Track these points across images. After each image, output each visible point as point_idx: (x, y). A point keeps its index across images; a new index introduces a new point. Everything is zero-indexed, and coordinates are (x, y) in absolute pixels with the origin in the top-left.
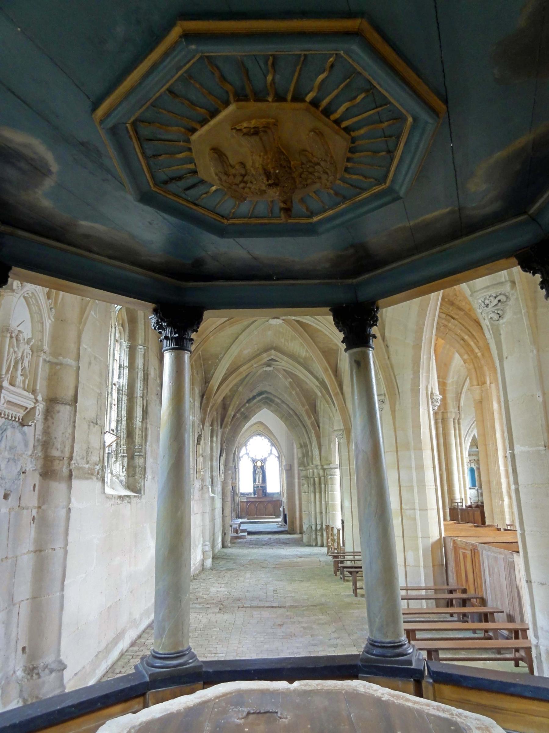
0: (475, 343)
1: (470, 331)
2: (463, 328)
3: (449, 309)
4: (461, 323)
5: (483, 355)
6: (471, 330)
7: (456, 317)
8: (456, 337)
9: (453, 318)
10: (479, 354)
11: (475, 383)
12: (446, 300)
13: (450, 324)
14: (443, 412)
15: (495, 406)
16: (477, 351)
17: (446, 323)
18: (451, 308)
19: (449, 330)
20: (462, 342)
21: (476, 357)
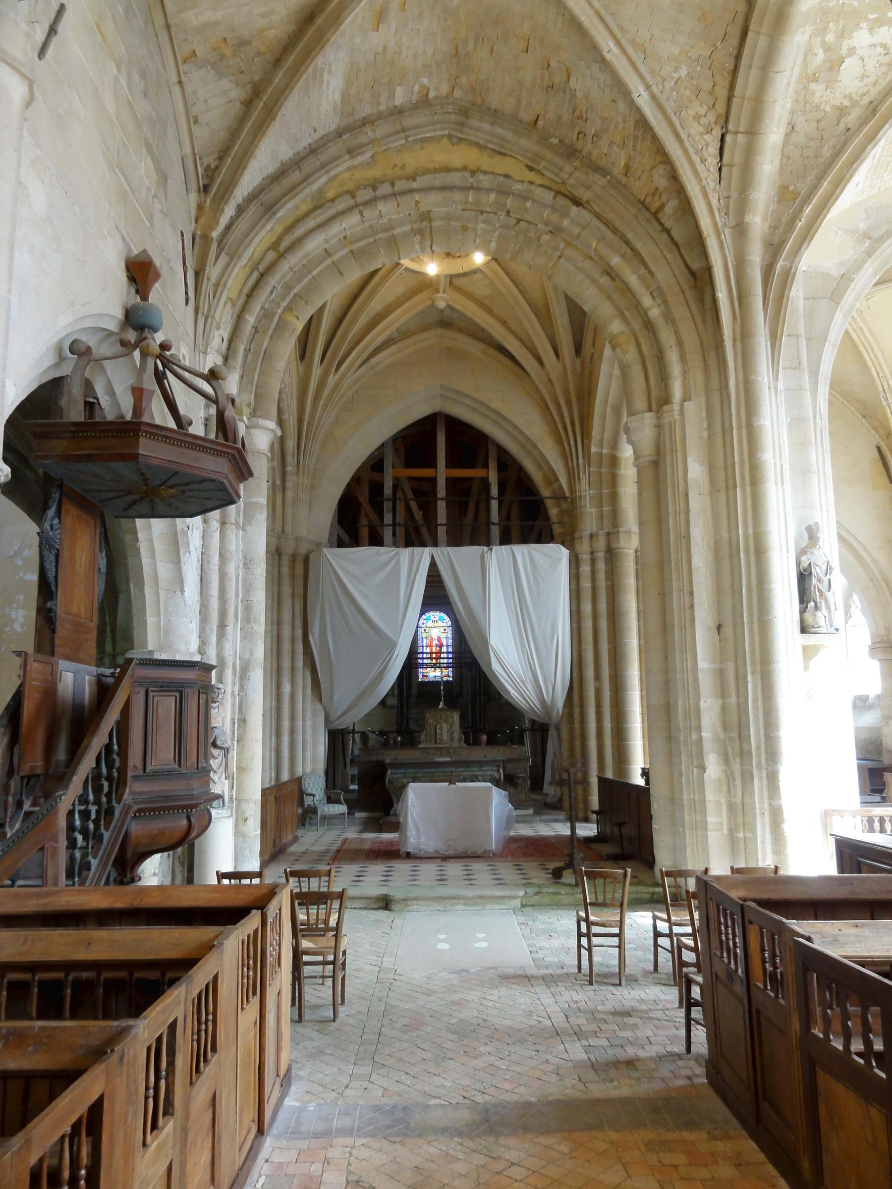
0: (642, 279)
1: (627, 243)
2: (608, 233)
3: (561, 169)
4: (598, 216)
5: (668, 315)
6: (630, 236)
7: (585, 195)
8: (588, 265)
9: (577, 202)
10: (655, 313)
11: (640, 403)
12: (555, 141)
13: (566, 223)
14: (608, 534)
15: (696, 470)
16: (647, 301)
17: (554, 218)
18: (568, 168)
19: (568, 244)
20: (604, 280)
21: (649, 325)
